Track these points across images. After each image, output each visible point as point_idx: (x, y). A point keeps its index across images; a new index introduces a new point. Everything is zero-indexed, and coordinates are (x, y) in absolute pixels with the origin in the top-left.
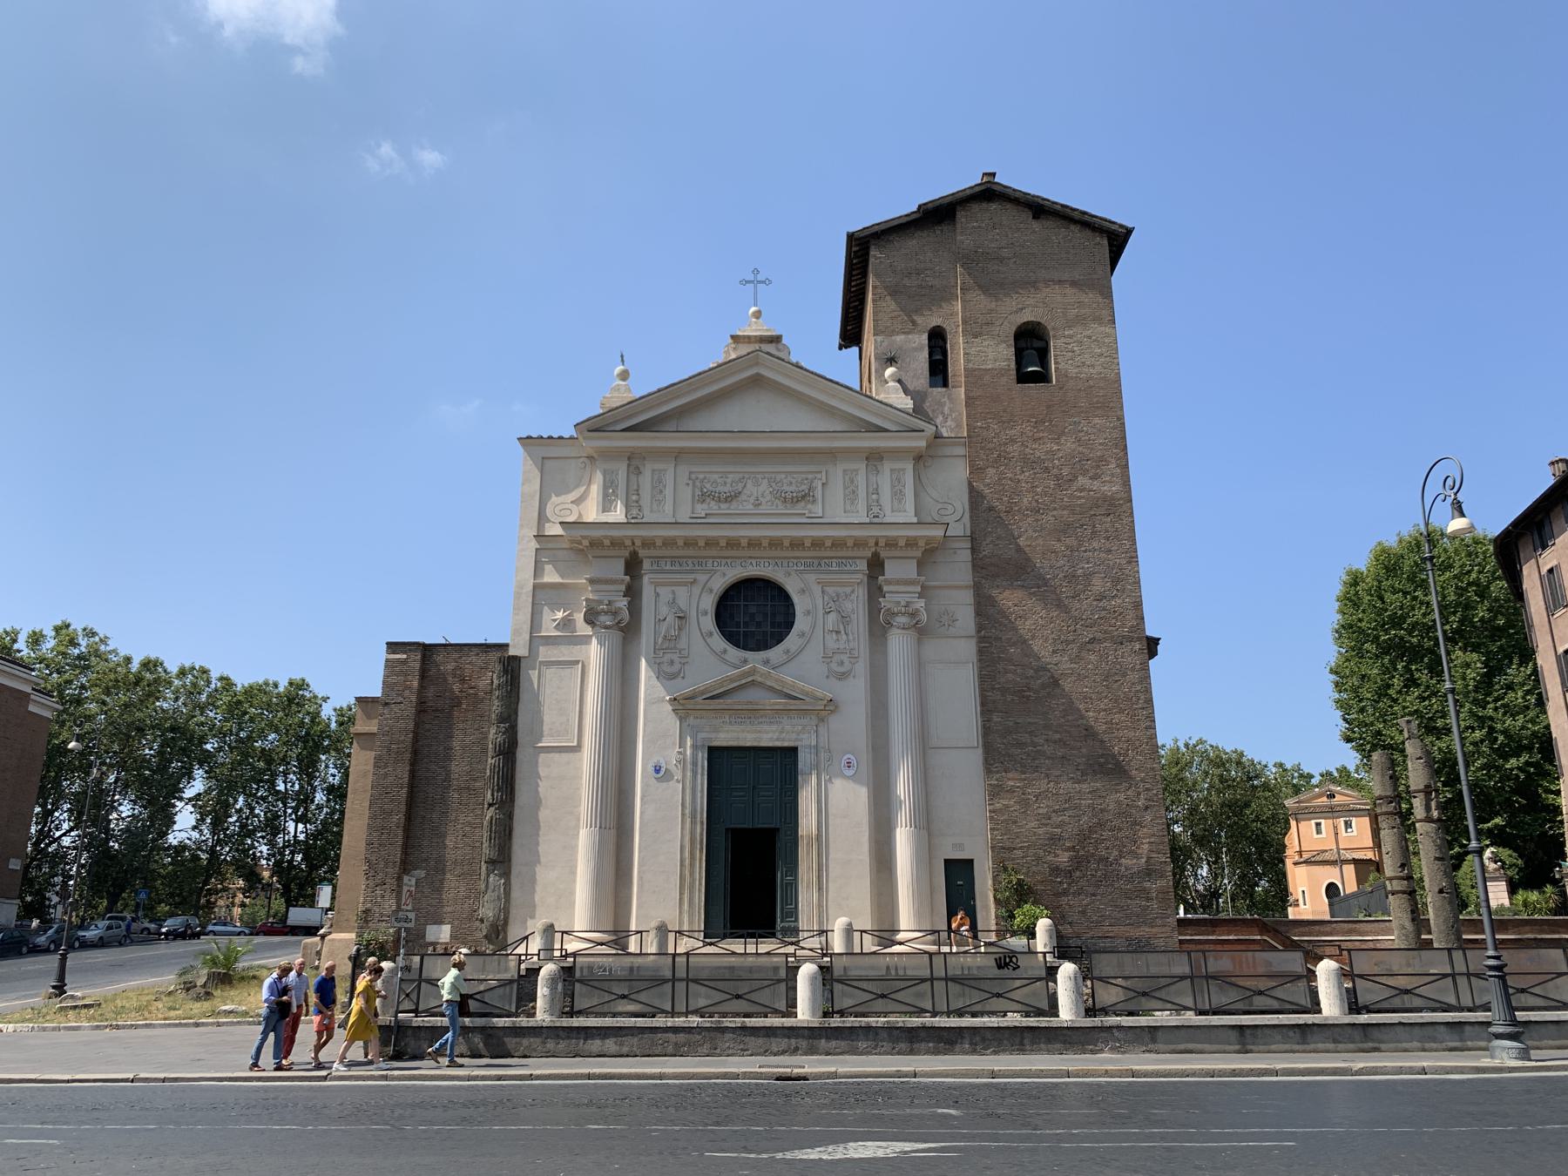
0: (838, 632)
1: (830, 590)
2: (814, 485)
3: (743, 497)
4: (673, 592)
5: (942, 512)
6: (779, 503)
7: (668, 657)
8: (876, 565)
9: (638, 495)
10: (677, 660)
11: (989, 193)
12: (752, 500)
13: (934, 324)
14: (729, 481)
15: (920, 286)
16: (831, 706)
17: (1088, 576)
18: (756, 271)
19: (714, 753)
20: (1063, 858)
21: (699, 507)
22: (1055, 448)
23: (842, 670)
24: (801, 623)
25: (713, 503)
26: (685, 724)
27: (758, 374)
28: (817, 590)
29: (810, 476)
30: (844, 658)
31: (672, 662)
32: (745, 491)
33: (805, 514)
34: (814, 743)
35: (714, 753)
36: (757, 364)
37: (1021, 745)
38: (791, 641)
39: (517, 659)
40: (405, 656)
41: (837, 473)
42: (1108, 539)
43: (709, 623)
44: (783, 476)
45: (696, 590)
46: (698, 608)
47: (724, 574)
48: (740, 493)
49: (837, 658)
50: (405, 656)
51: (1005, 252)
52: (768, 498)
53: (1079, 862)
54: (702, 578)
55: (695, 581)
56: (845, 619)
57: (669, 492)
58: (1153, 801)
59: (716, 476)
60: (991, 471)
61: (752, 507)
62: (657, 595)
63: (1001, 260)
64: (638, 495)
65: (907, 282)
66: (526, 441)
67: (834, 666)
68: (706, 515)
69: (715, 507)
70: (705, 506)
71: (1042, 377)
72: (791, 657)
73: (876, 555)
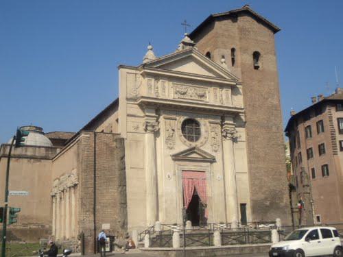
11: (246, 12)
18: (185, 21)
20: (268, 203)
21: (176, 96)
38: (202, 139)
41: (211, 89)
53: (271, 204)
63: (249, 32)
72: (203, 144)
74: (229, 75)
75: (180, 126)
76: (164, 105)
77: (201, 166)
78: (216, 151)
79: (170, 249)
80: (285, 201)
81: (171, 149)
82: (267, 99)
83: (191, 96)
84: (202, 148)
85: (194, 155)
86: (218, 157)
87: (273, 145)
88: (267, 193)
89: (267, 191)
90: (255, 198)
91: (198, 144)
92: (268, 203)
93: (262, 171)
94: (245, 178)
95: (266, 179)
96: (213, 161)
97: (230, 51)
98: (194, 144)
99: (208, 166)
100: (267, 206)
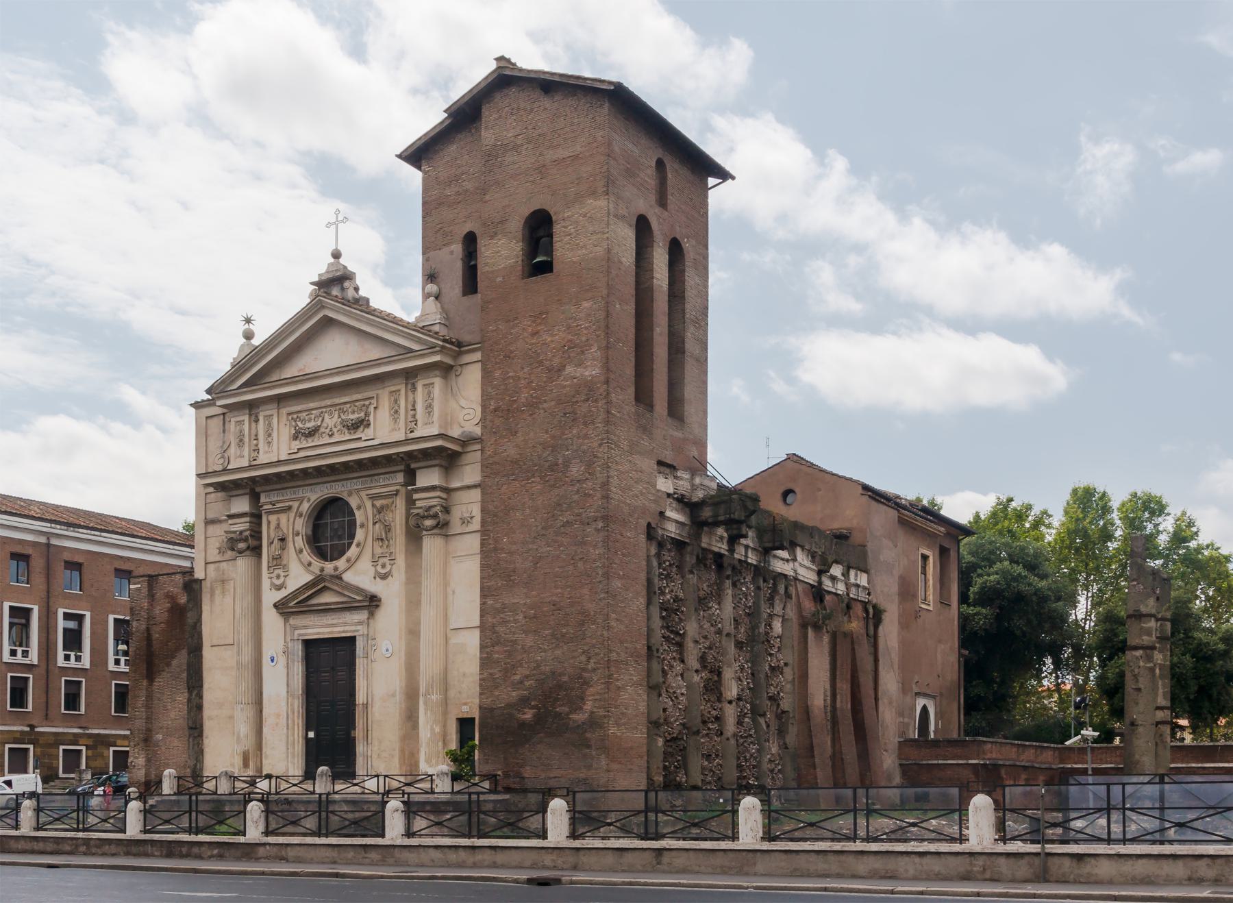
0: (382, 540)
1: (378, 503)
2: (369, 410)
3: (322, 430)
4: (278, 518)
5: (467, 417)
6: (346, 431)
7: (277, 572)
8: (411, 476)
9: (257, 439)
10: (282, 574)
12: (327, 431)
13: (467, 230)
14: (313, 417)
15: (458, 193)
16: (372, 603)
17: (567, 464)
19: (308, 644)
20: (528, 715)
21: (296, 445)
22: (549, 339)
23: (383, 571)
24: (360, 535)
25: (303, 438)
26: (288, 624)
27: (325, 316)
28: (368, 504)
29: (367, 403)
30: (386, 560)
31: (278, 577)
32: (324, 425)
33: (361, 438)
34: (366, 633)
35: (308, 644)
36: (323, 307)
37: (505, 622)
38: (353, 551)
39: (200, 581)
40: (139, 586)
41: (384, 396)
42: (585, 423)
43: (300, 541)
44: (348, 406)
45: (292, 515)
46: (293, 529)
47: (309, 500)
48: (319, 426)
49: (382, 561)
50: (139, 586)
51: (519, 140)
52: (339, 427)
53: (539, 719)
54: (295, 505)
55: (290, 508)
56: (388, 528)
57: (275, 434)
58: (600, 664)
59: (304, 414)
60: (497, 374)
61: (327, 436)
62: (269, 522)
63: (516, 148)
64: (257, 439)
65: (447, 192)
66: (191, 405)
67: (379, 569)
68: (298, 449)
69: (305, 442)
70: (297, 442)
71: (545, 268)
72: (351, 563)
73: (408, 466)
74: (419, 341)
75: (301, 525)
76: (266, 479)
77: (346, 624)
78: (384, 577)
79: (379, 841)
80: (589, 706)
81: (279, 588)
82: (562, 368)
83: (331, 436)
84: (348, 577)
85: (327, 598)
86: (391, 592)
87: (568, 523)
88: (527, 684)
89: (527, 677)
90: (488, 702)
91: (341, 563)
92: (528, 715)
93: (520, 617)
94: (472, 642)
95: (529, 641)
96: (372, 603)
97: (457, 249)
98: (329, 567)
99: (360, 623)
100: (523, 725)
